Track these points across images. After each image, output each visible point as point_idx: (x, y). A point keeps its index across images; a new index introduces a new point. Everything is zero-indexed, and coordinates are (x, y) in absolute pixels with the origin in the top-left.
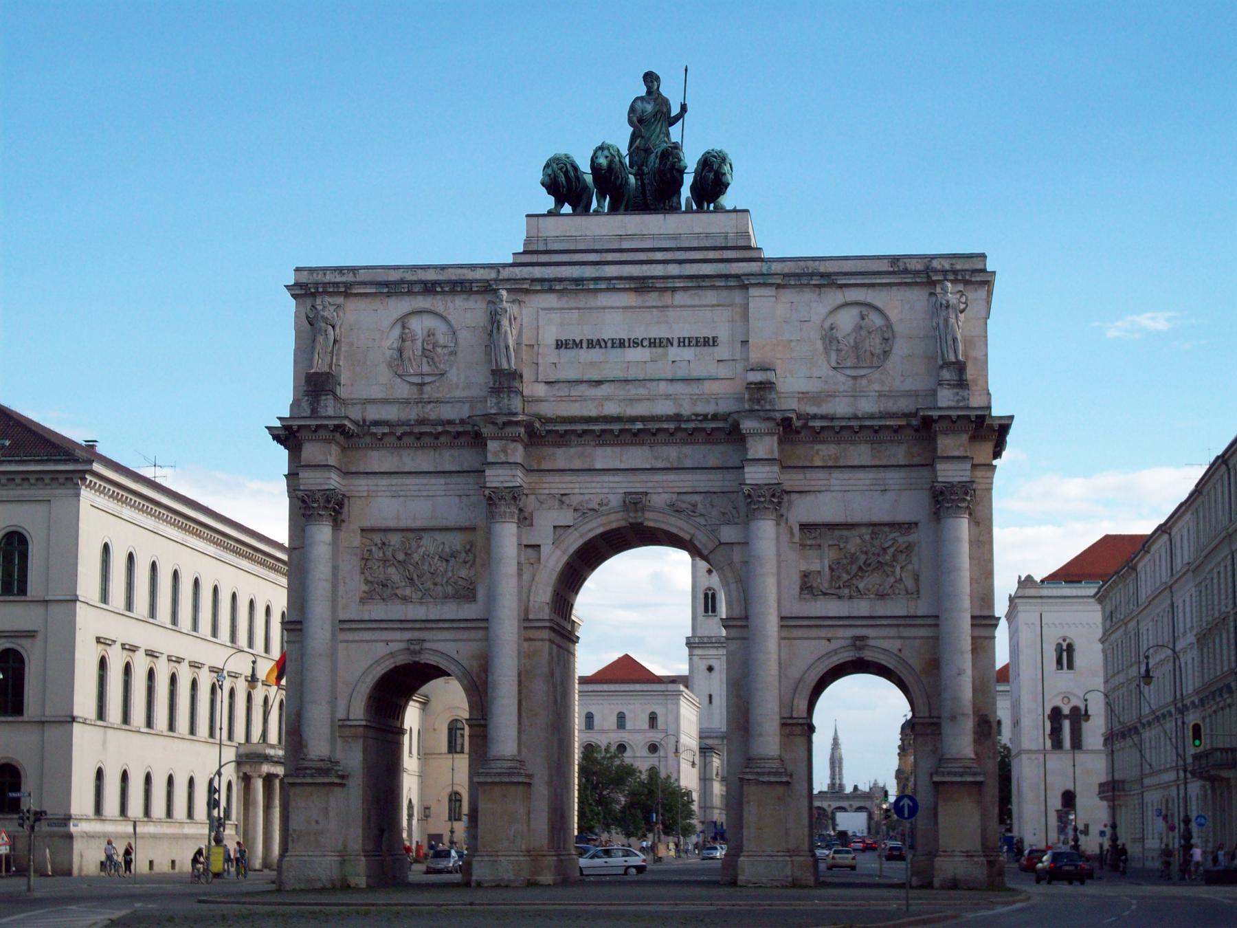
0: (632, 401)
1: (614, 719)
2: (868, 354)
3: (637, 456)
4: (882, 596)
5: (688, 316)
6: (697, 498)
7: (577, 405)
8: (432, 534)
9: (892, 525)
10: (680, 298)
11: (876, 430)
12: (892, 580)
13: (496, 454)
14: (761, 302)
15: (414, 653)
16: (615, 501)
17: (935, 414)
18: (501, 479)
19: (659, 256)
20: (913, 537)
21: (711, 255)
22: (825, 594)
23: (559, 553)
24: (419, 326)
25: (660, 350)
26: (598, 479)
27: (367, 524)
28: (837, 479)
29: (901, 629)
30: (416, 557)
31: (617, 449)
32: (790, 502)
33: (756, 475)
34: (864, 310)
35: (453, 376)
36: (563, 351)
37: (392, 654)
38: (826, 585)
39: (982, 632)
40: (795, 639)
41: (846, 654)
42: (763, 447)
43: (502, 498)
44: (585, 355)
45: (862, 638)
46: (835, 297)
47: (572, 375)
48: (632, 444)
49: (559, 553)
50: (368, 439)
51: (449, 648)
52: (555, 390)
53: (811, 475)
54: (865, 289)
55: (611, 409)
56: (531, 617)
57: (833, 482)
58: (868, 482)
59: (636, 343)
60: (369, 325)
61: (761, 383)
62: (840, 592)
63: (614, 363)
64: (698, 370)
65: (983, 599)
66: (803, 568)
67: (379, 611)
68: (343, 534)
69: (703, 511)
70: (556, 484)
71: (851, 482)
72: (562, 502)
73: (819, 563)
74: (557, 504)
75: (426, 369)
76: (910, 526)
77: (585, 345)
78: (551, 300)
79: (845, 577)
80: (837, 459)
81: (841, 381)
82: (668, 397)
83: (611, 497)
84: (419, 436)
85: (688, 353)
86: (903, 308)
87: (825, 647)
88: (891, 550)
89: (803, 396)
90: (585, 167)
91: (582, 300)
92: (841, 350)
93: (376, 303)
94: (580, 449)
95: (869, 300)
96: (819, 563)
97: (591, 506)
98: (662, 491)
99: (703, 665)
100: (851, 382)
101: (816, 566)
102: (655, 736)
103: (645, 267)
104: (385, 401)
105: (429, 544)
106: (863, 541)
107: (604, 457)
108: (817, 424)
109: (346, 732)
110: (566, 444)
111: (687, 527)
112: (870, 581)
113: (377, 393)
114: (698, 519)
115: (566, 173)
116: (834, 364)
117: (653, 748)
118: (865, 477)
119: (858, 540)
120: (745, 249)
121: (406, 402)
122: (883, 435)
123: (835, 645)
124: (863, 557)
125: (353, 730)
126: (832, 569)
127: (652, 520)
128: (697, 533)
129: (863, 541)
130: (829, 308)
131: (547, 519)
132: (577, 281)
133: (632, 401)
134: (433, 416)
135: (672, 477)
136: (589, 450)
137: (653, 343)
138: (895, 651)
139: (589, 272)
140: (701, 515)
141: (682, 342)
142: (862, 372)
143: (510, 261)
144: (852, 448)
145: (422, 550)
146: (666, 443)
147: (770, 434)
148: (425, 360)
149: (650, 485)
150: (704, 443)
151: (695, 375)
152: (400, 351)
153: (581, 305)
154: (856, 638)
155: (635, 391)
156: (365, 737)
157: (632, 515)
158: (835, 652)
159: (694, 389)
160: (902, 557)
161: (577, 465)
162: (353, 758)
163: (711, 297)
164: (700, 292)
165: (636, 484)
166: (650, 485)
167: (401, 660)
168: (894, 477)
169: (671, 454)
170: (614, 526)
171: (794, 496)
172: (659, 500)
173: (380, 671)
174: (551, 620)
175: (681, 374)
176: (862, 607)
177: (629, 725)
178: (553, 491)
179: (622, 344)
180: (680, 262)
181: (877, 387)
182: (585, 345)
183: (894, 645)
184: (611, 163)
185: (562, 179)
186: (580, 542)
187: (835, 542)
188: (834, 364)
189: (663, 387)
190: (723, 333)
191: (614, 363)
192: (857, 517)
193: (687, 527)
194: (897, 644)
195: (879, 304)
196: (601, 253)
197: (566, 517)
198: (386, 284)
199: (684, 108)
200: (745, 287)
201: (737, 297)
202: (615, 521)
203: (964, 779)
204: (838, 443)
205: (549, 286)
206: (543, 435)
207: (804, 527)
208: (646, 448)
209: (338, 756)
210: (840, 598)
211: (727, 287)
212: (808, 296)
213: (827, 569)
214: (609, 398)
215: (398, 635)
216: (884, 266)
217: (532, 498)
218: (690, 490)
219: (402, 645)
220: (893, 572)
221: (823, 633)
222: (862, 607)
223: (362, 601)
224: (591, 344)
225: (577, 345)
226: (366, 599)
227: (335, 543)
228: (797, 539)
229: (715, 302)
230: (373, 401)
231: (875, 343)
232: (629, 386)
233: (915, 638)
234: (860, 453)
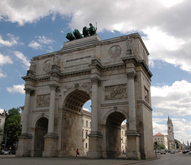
1: (155, 139)
2: (117, 54)
3: (77, 78)
4: (120, 99)
5: (86, 53)
6: (87, 84)
7: (69, 71)
8: (47, 95)
9: (122, 85)
10: (85, 50)
11: (118, 66)
12: (122, 95)
13: (51, 79)
14: (98, 48)
15: (42, 115)
16: (74, 86)
17: (125, 59)
18: (52, 83)
19: (82, 44)
21: (91, 42)
22: (109, 99)
23: (64, 96)
24: (48, 62)
25: (82, 59)
26: (71, 83)
27: (38, 95)
28: (112, 77)
29: (124, 105)
30: (44, 99)
31: (74, 77)
32: (103, 83)
33: (93, 76)
34: (116, 47)
36: (67, 62)
37: (40, 116)
38: (110, 98)
39: (139, 104)
40: (104, 108)
41: (113, 111)
42: (94, 71)
43: (52, 86)
44: (70, 62)
45: (117, 107)
46: (111, 45)
47: (68, 67)
48: (76, 76)
49: (64, 96)
50: (39, 81)
51: (47, 114)
52: (65, 69)
53: (106, 77)
54: (116, 43)
55: (74, 70)
56: (60, 108)
57: (111, 78)
58: (117, 77)
59: (78, 59)
60: (41, 63)
61: (94, 60)
62: (112, 99)
63: (74, 63)
65: (140, 97)
66: (106, 95)
67: (39, 109)
69: (88, 86)
70: (65, 84)
71: (114, 77)
72: (65, 87)
73: (108, 94)
74: (64, 88)
75: (48, 69)
76: (125, 85)
77: (70, 61)
78: (66, 55)
79: (113, 96)
80: (111, 74)
81: (112, 59)
82: (83, 67)
83: (73, 86)
84: (45, 79)
85: (86, 59)
86: (123, 45)
87: (109, 110)
88: (122, 89)
89: (106, 63)
90: (73, 33)
91: (70, 54)
92: (112, 54)
93: (42, 60)
94: (69, 78)
95: (117, 45)
96: (108, 94)
97: (70, 88)
98: (81, 83)
99: (169, 134)
100: (114, 59)
101: (108, 94)
102: (162, 140)
103: (80, 46)
104: (42, 75)
105: (47, 97)
106: (117, 88)
107: (72, 79)
108: (107, 67)
109: (33, 129)
110: (67, 77)
111: (85, 89)
112: (118, 96)
113: (41, 74)
114: (87, 88)
115: (69, 35)
116: (111, 57)
117: (162, 142)
118: (116, 76)
119: (116, 89)
120: (96, 40)
122: (120, 67)
123: (111, 109)
124: (116, 92)
125: (34, 129)
126: (111, 94)
127: (80, 89)
128: (87, 90)
129: (117, 88)
130: (110, 47)
131: (63, 90)
132: (69, 51)
135: (83, 81)
136: (70, 78)
137: (81, 59)
138: (123, 110)
140: (88, 87)
141: (85, 58)
142: (116, 57)
143: (61, 50)
144: (114, 71)
145: (45, 98)
146: (82, 75)
147: (95, 68)
148: (48, 68)
149: (79, 83)
150: (88, 74)
151: (87, 63)
152: (45, 67)
153: (70, 54)
154: (114, 107)
155: (77, 67)
156: (35, 130)
157: (76, 88)
158: (111, 110)
160: (124, 91)
161: (68, 81)
163: (90, 49)
164: (88, 49)
165: (76, 83)
166: (79, 83)
167: (41, 117)
168: (122, 76)
169: (83, 77)
170: (73, 91)
172: (80, 85)
173: (38, 119)
174: (63, 108)
176: (116, 101)
177: (159, 139)
178: (64, 86)
179: (76, 60)
180: (86, 45)
181: (119, 60)
182: (70, 61)
183: (122, 108)
184: (76, 32)
185: (69, 36)
186: (68, 94)
187: (112, 89)
188: (111, 57)
189: (82, 66)
191: (74, 63)
192: (115, 84)
193: (85, 89)
194: (123, 108)
195: (119, 45)
196: (74, 46)
197: (66, 90)
198: (43, 57)
199: (96, 28)
200: (95, 46)
201: (94, 48)
202: (73, 90)
203: (132, 135)
204: (111, 70)
205: (65, 53)
206: (61, 76)
207: (105, 87)
208: (79, 76)
210: (112, 100)
211: (93, 47)
212: (107, 46)
213: (110, 95)
214: (74, 69)
215: (41, 113)
216: (120, 38)
217: (61, 87)
218: (86, 83)
219: (41, 114)
220: (122, 94)
221: (109, 107)
222: (116, 101)
223: (36, 107)
224: (71, 60)
225: (69, 61)
226: (36, 107)
228: (104, 89)
229: (91, 50)
230: (40, 75)
231: (119, 52)
232: (77, 66)
233: (126, 106)
234: (116, 72)
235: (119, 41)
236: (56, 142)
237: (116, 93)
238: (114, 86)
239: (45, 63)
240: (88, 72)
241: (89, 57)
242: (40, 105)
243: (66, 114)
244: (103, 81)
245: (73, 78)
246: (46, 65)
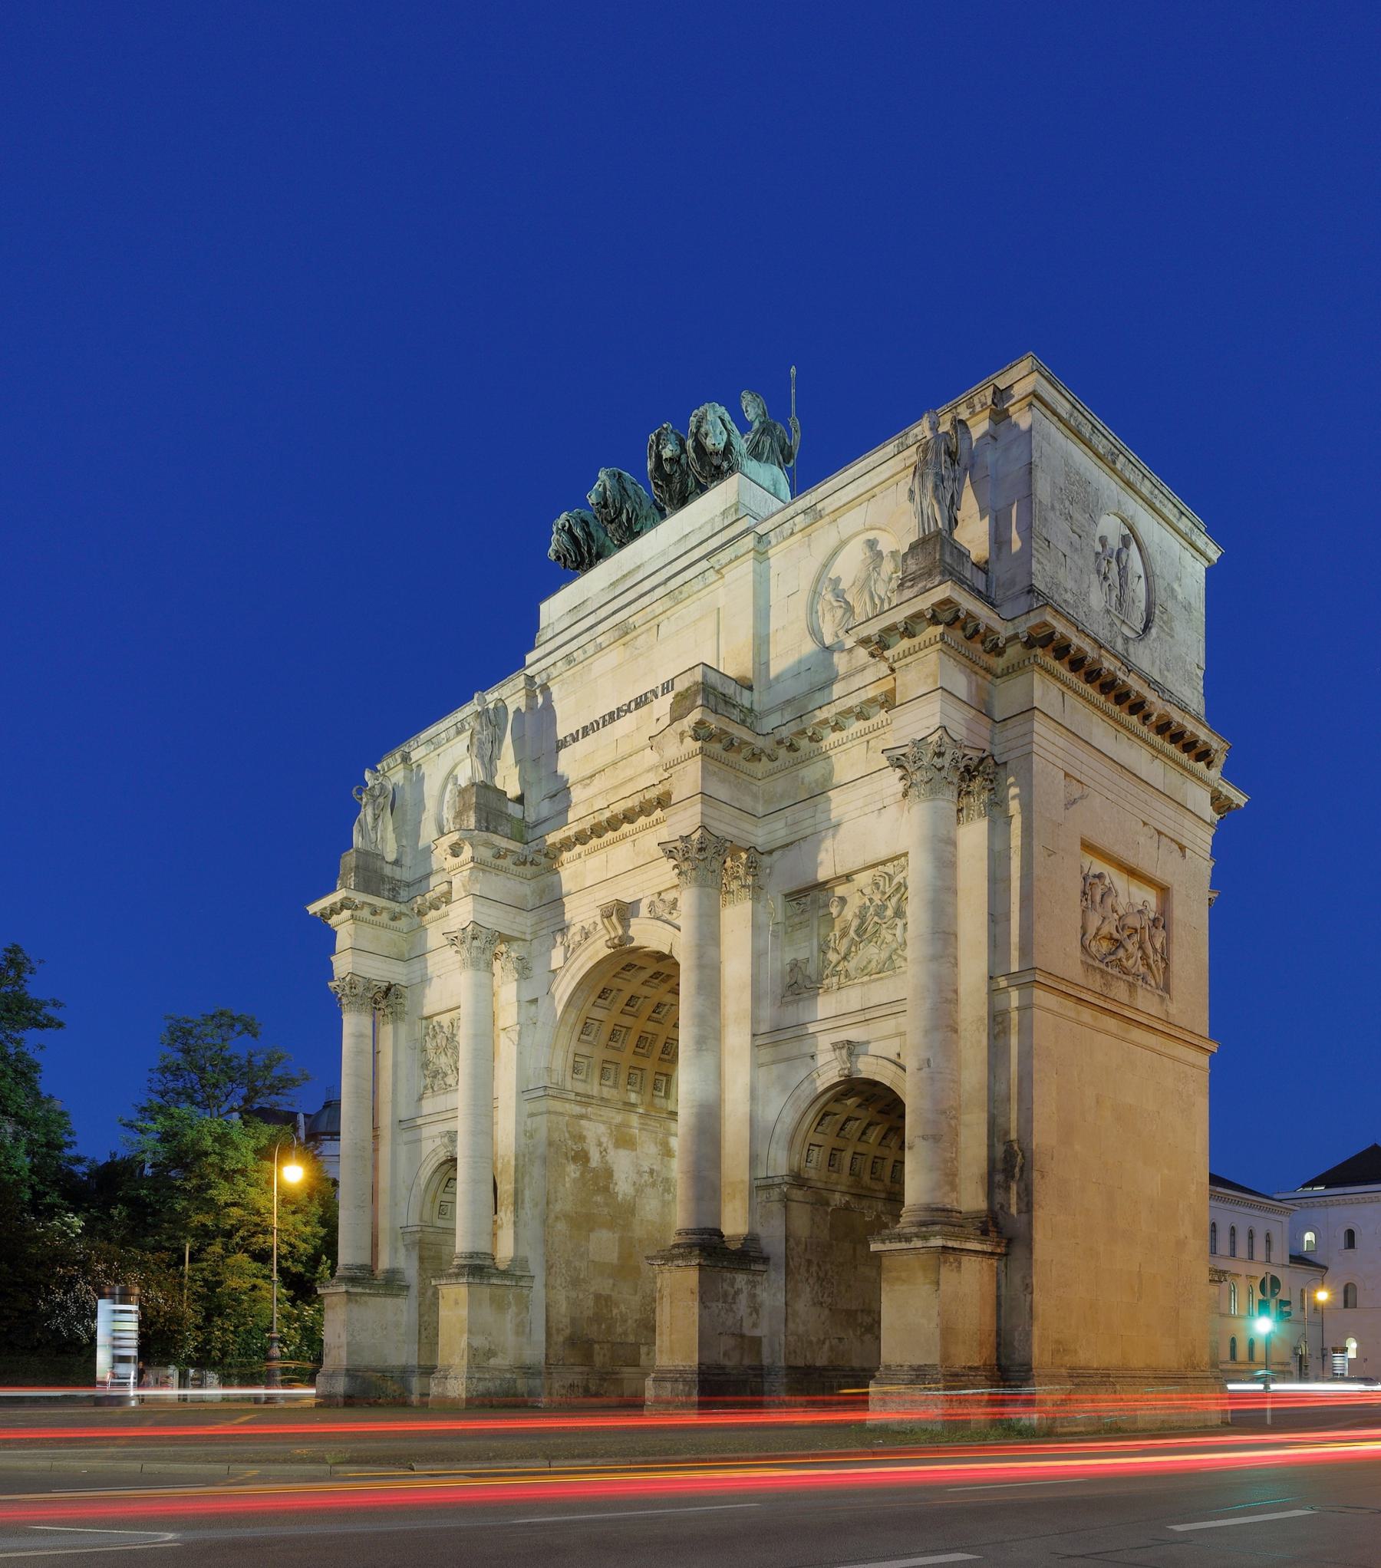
138: (894, 1057)
171: (776, 855)
186: (574, 984)
213: (815, 953)
222: (851, 998)
236: (513, 1309)
238: (848, 877)
242: (434, 1077)
243: (583, 1122)
244: (770, 852)
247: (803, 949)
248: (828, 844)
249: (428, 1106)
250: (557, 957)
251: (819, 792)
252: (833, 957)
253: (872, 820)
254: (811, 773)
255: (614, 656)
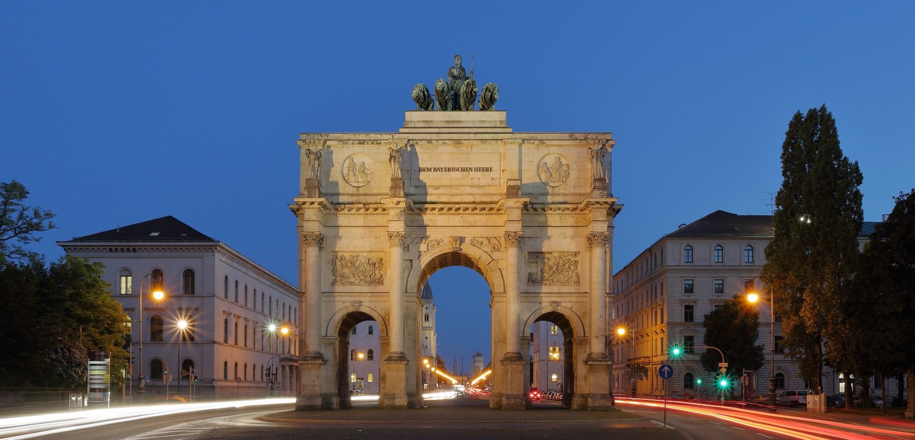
0: (453, 195)
3: (456, 220)
16: (446, 241)
20: (578, 258)
25: (465, 173)
35: (372, 183)
55: (444, 199)
59: (454, 169)
64: (483, 182)
68: (323, 254)
75: (360, 180)
101: (534, 271)
121: (352, 195)
132: (429, 141)
133: (453, 195)
134: (364, 201)
135: (472, 229)
137: (463, 170)
139: (434, 136)
141: (477, 170)
154: (552, 302)
159: (481, 191)
160: (572, 268)
162: (330, 354)
167: (351, 309)
169: (470, 219)
172: (467, 240)
175: (475, 183)
179: (449, 170)
183: (569, 305)
189: (467, 188)
190: (495, 165)
209: (323, 351)
215: (348, 299)
222: (555, 289)
224: (435, 170)
227: (320, 256)
235: (566, 146)
237: (554, 269)
238: (551, 253)
239: (347, 161)
240: (487, 207)
241: (487, 170)
245: (443, 217)
246: (353, 167)
247: (533, 269)
248: (546, 241)
249: (339, 288)
250: (423, 247)
251: (545, 226)
252: (546, 275)
253: (560, 238)
254: (540, 219)
255: (449, 149)
